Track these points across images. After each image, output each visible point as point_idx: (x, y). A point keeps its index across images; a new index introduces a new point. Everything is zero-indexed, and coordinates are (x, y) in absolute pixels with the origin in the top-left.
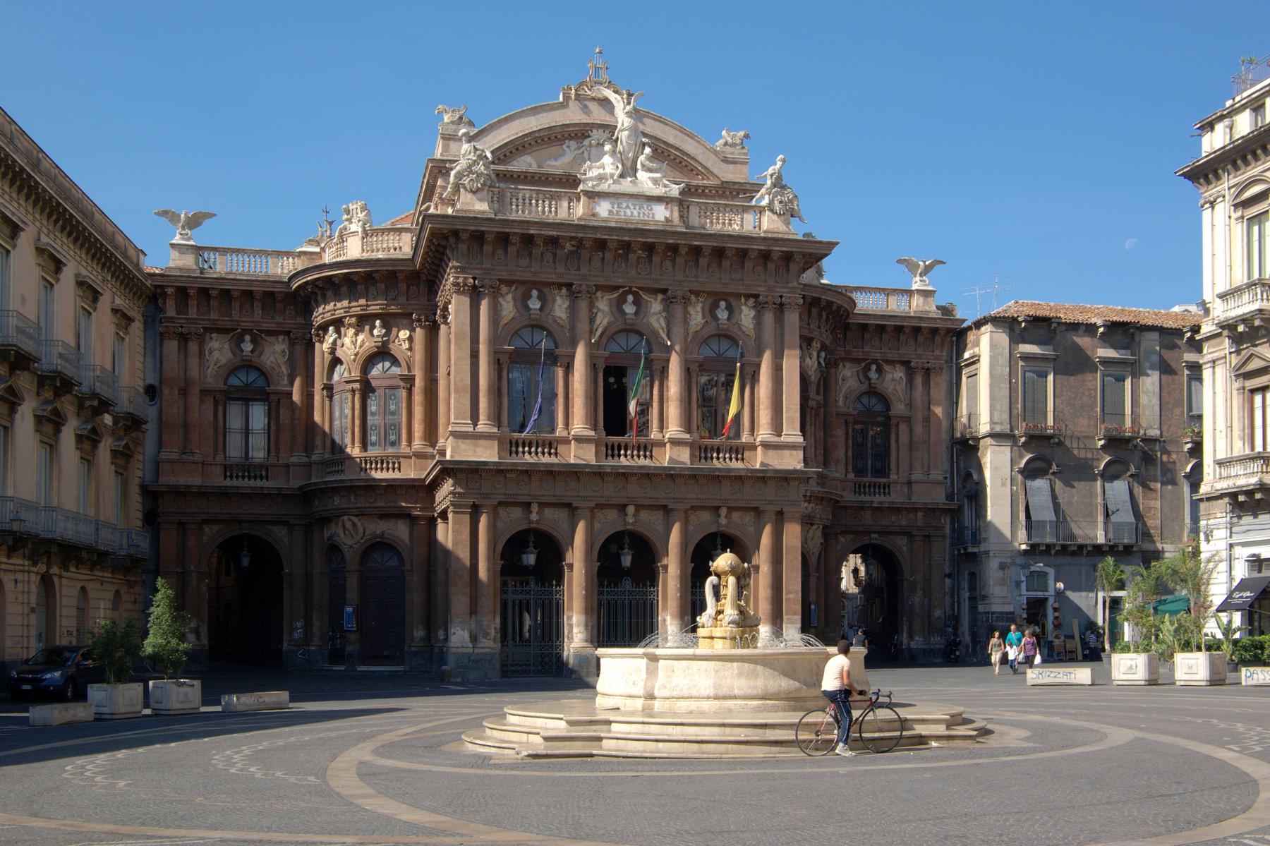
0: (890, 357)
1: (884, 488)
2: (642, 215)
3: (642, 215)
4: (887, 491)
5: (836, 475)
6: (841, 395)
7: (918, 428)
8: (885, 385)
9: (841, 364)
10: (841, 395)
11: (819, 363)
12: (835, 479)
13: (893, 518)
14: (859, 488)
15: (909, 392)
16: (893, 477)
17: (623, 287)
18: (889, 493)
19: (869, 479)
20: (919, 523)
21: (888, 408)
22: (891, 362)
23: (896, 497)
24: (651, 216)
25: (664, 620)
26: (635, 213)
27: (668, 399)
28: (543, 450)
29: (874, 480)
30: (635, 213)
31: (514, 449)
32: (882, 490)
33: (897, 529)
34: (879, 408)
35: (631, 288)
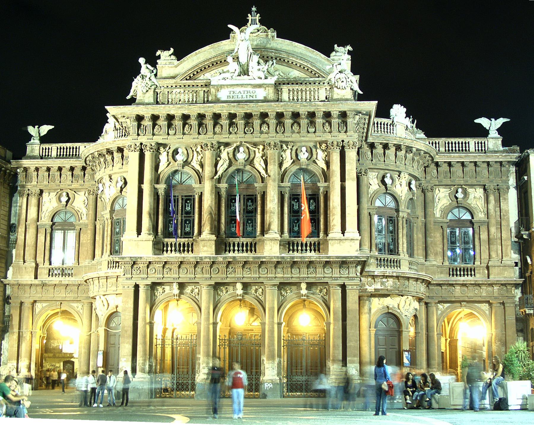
0: (470, 183)
1: (471, 271)
2: (248, 97)
3: (248, 97)
4: (473, 273)
5: (434, 263)
6: (438, 210)
7: (493, 230)
8: (469, 201)
9: (437, 189)
10: (438, 210)
11: (410, 188)
12: (434, 265)
13: (476, 292)
14: (453, 272)
15: (486, 205)
16: (477, 263)
17: (236, 142)
18: (474, 275)
19: (458, 264)
20: (496, 295)
21: (473, 218)
22: (472, 186)
23: (480, 277)
24: (254, 97)
25: (263, 360)
26: (244, 96)
27: (267, 212)
28: (167, 249)
29: (463, 265)
30: (244, 96)
31: (165, 249)
32: (469, 273)
33: (480, 299)
34: (467, 217)
35: (241, 142)
